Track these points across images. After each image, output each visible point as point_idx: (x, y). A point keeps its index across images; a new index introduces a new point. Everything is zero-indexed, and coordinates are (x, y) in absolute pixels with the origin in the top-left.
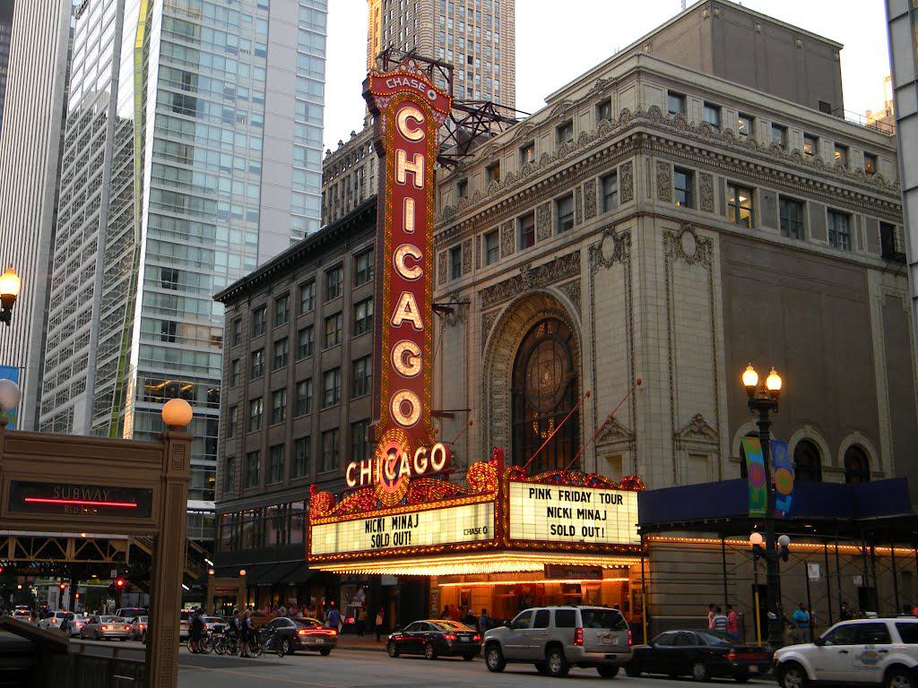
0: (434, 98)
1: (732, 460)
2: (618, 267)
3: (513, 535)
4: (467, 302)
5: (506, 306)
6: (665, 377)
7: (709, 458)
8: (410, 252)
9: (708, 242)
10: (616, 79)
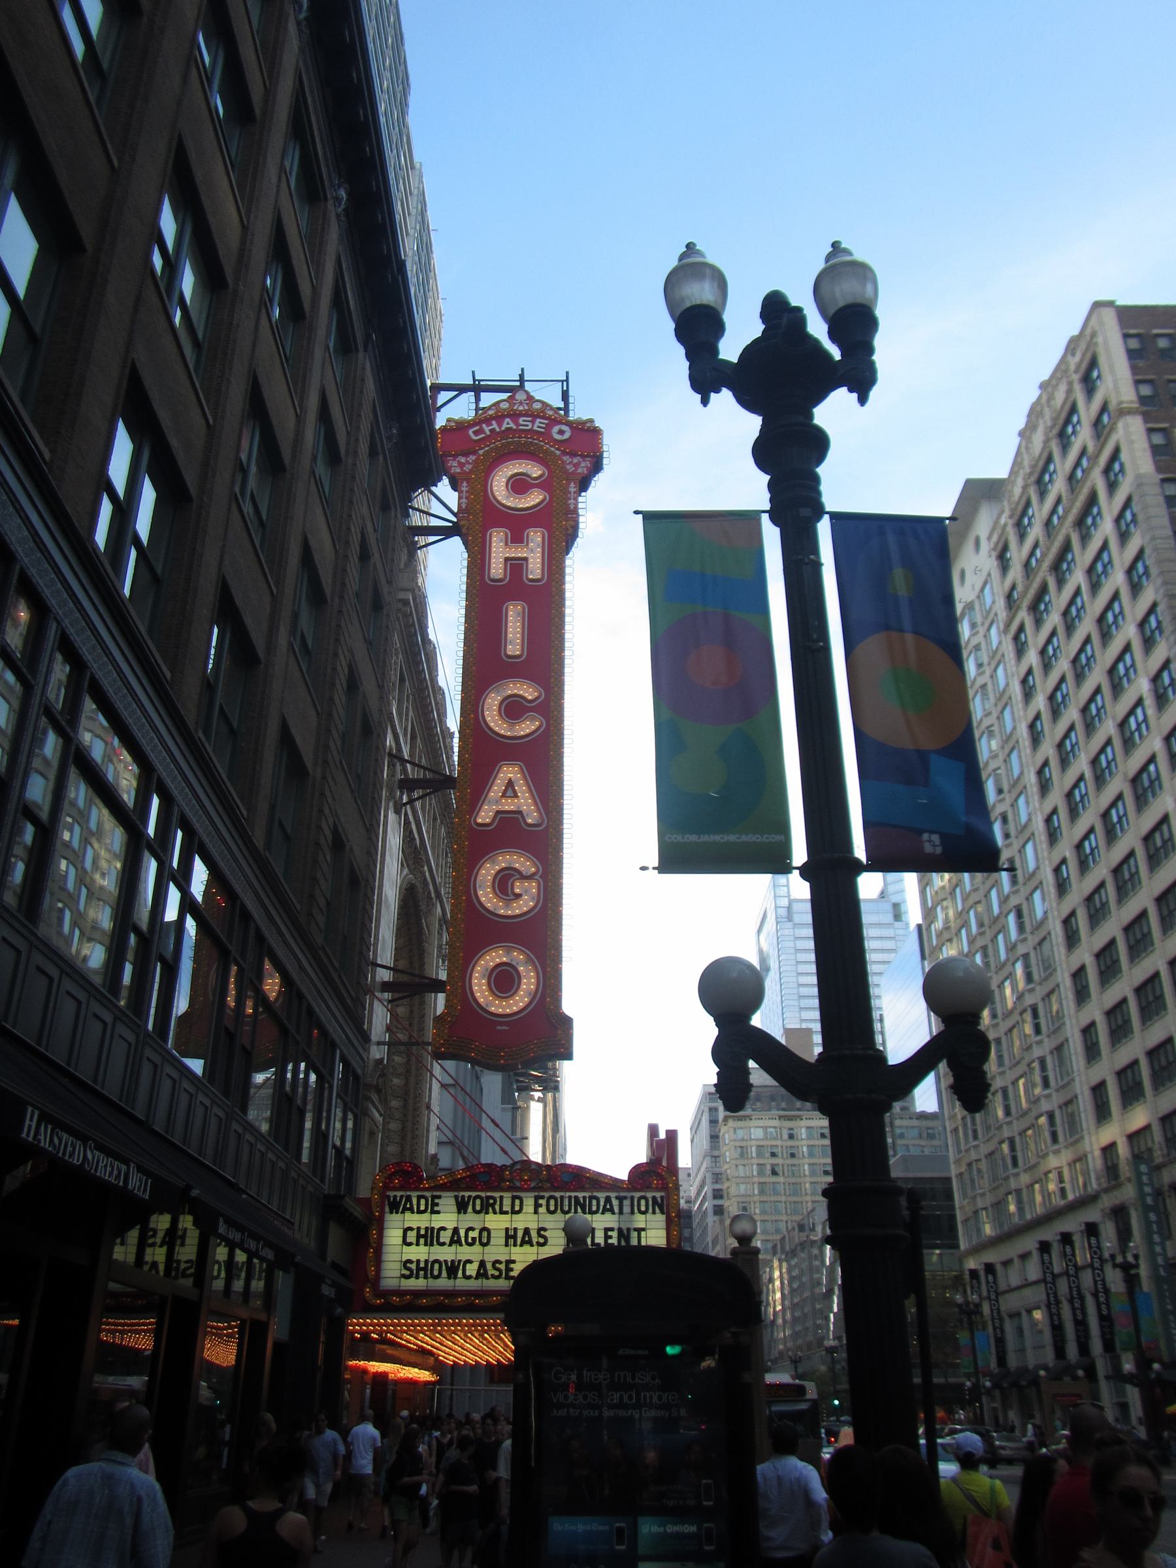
0: (567, 436)
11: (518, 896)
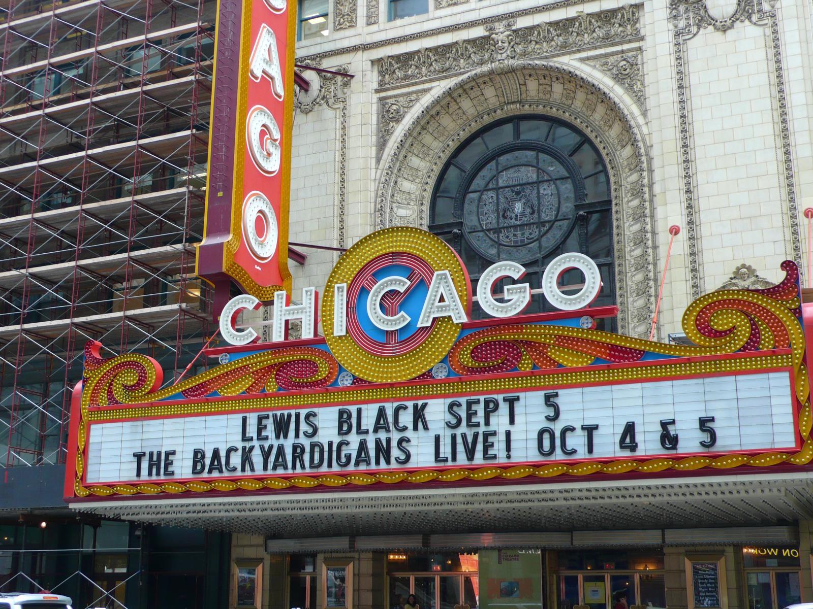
4: (346, 75)
5: (440, 88)
11: (269, 154)
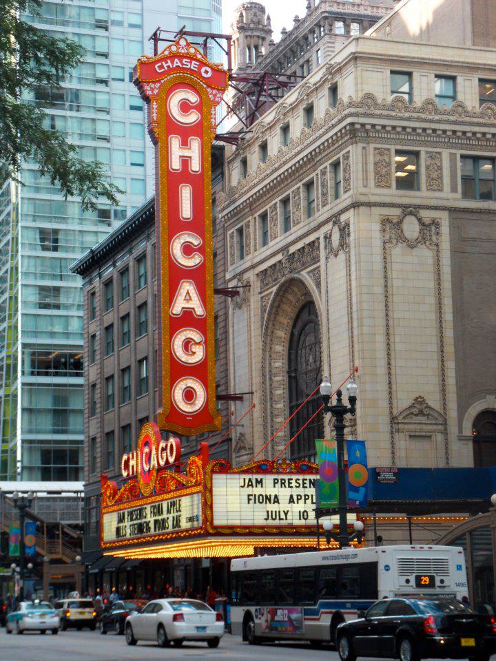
0: (210, 75)
1: (461, 438)
2: (342, 256)
3: (217, 522)
4: (247, 286)
5: (275, 289)
6: (383, 363)
7: (433, 438)
8: (188, 239)
9: (436, 223)
10: (340, 64)
11: (194, 353)
